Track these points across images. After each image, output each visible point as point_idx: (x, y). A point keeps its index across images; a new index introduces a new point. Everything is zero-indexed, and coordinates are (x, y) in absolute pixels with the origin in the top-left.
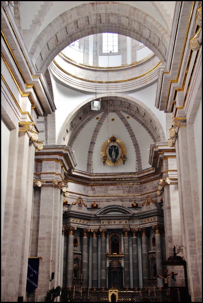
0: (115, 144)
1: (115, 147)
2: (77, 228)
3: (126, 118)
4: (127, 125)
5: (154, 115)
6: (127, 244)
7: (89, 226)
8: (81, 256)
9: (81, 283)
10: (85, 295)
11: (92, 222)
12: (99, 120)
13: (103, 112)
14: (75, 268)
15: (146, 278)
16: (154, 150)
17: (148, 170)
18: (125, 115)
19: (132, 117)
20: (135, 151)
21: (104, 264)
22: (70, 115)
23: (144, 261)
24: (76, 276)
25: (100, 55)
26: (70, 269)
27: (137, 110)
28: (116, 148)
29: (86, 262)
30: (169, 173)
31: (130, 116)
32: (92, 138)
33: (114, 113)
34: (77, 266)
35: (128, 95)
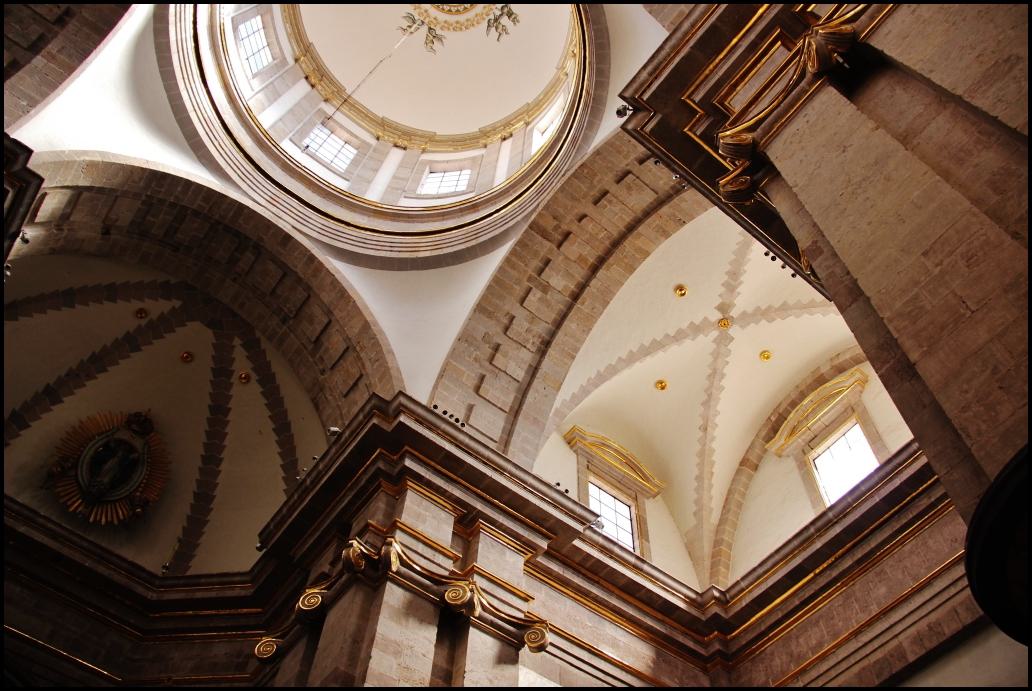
0: (138, 443)
1: (132, 449)
3: (234, 379)
4: (219, 411)
5: (391, 352)
12: (140, 326)
13: (177, 303)
16: (375, 421)
17: (225, 579)
18: (241, 364)
19: (259, 382)
20: (188, 517)
22: (101, 153)
25: (291, 140)
27: (318, 338)
28: (132, 456)
30: (399, 535)
31: (254, 377)
32: (67, 375)
33: (209, 333)
35: (330, 259)
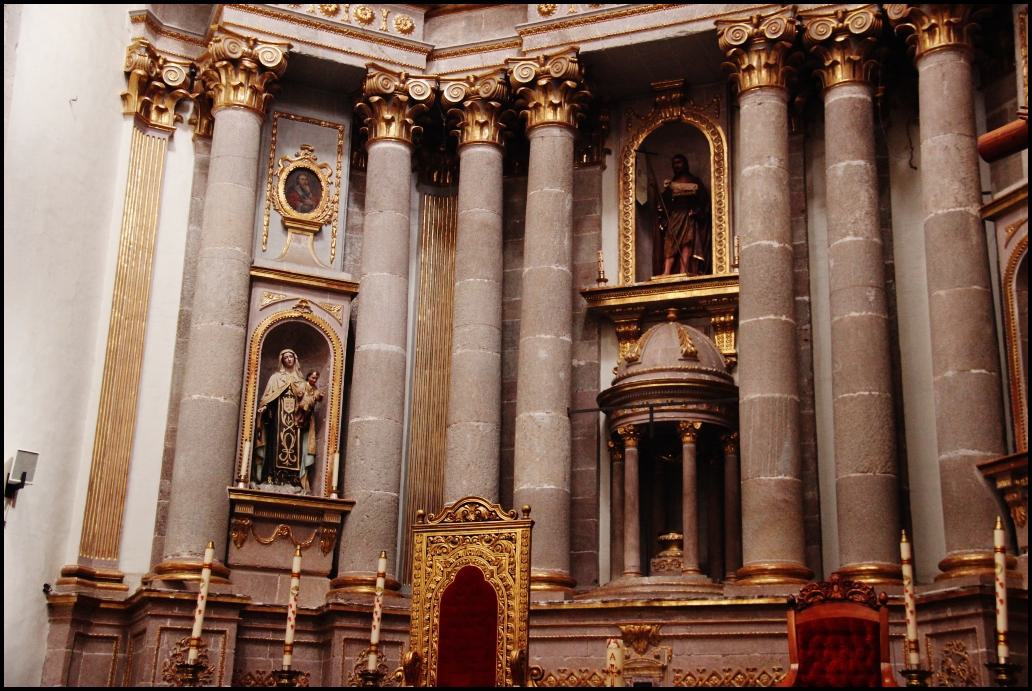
2: (290, 57)
6: (759, 158)
7: (432, 55)
8: (341, 306)
9: (333, 544)
10: (347, 641)
11: (463, 24)
14: (274, 405)
15: (971, 452)
21: (543, 354)
23: (942, 293)
24: (269, 464)
26: (195, 397)
29: (378, 351)
34: (303, 386)
